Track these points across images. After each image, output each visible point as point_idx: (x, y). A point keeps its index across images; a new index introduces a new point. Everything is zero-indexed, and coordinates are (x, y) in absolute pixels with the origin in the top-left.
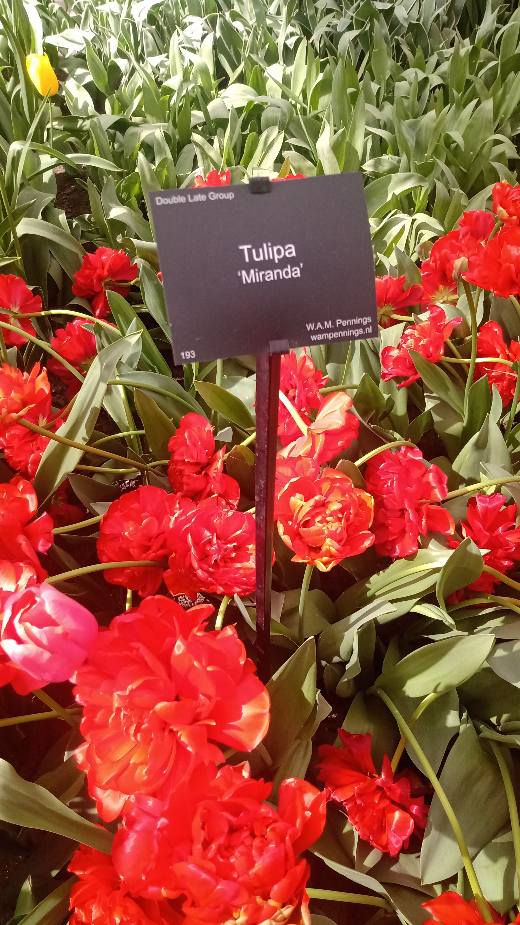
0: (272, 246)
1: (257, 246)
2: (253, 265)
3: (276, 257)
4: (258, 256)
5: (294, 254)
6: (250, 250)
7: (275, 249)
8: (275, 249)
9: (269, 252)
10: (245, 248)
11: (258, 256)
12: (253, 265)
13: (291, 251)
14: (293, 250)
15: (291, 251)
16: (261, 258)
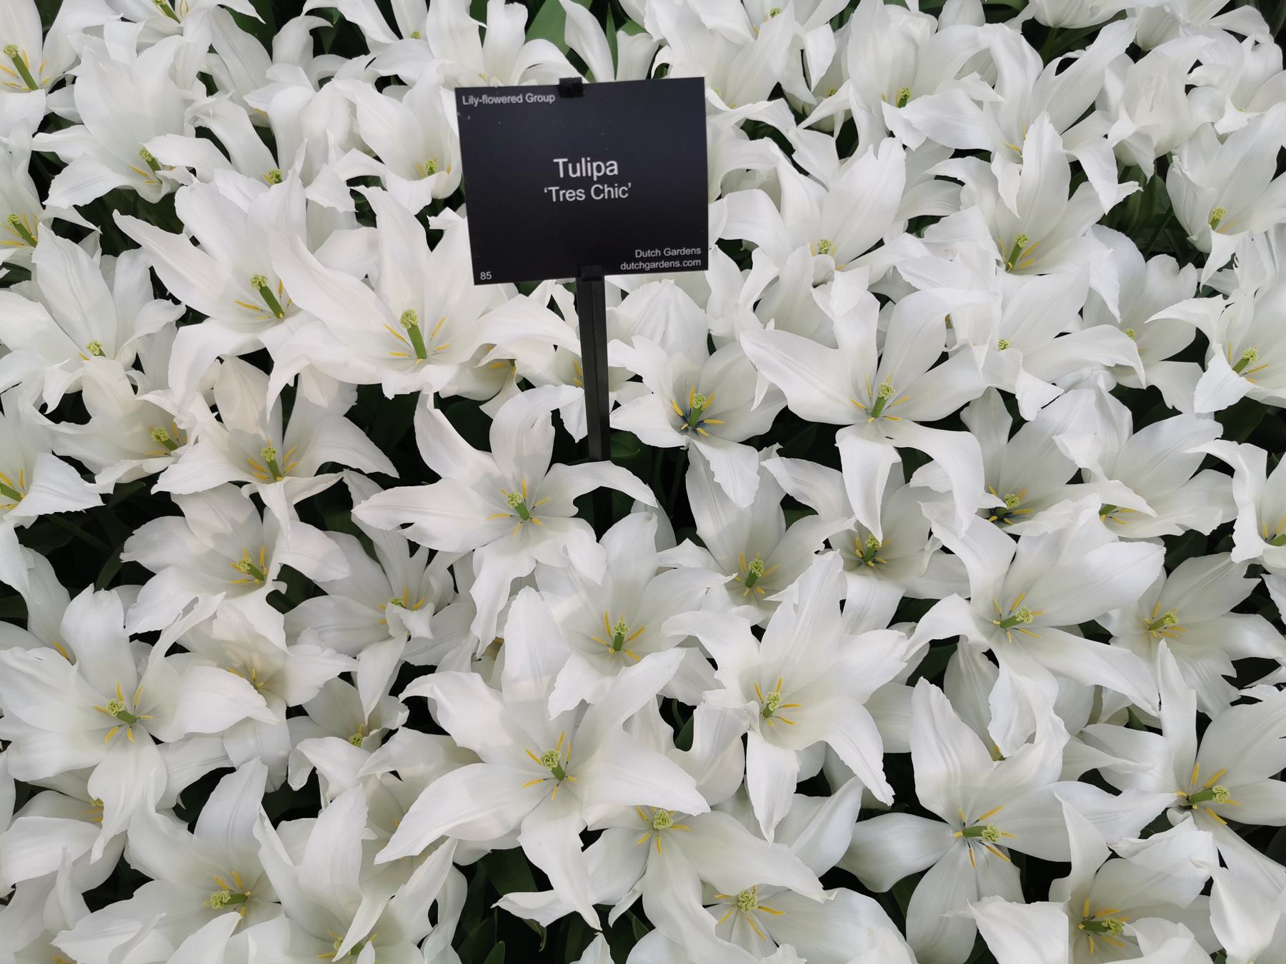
0: (591, 162)
1: (575, 160)
2: (568, 183)
3: (595, 174)
4: (574, 172)
5: (616, 172)
6: (565, 165)
7: (595, 165)
8: (595, 165)
10: (561, 161)
11: (574, 172)
12: (568, 183)
13: (613, 168)
14: (615, 167)
15: (613, 168)
16: (578, 174)
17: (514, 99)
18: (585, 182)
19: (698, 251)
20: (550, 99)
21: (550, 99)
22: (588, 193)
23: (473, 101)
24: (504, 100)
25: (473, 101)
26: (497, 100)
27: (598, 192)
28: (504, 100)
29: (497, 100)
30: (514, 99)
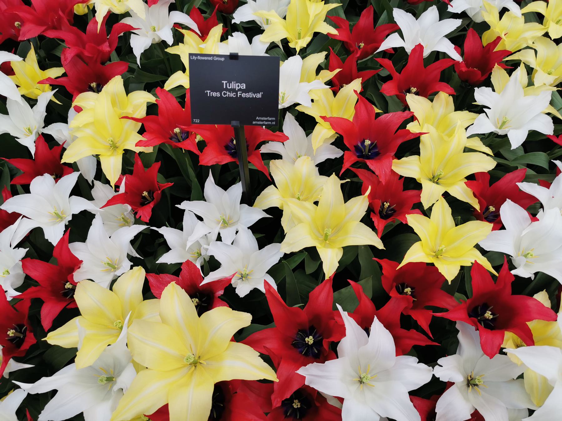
1: (230, 82)
2: (227, 89)
3: (237, 88)
6: (226, 84)
9: (234, 85)
10: (225, 82)
13: (244, 86)
14: (245, 86)
17: (209, 58)
18: (233, 90)
19: (274, 119)
20: (223, 59)
21: (223, 59)
22: (221, 94)
23: (194, 58)
24: (206, 58)
25: (194, 58)
26: (203, 58)
27: (225, 94)
28: (206, 58)
29: (203, 58)
30: (209, 58)
